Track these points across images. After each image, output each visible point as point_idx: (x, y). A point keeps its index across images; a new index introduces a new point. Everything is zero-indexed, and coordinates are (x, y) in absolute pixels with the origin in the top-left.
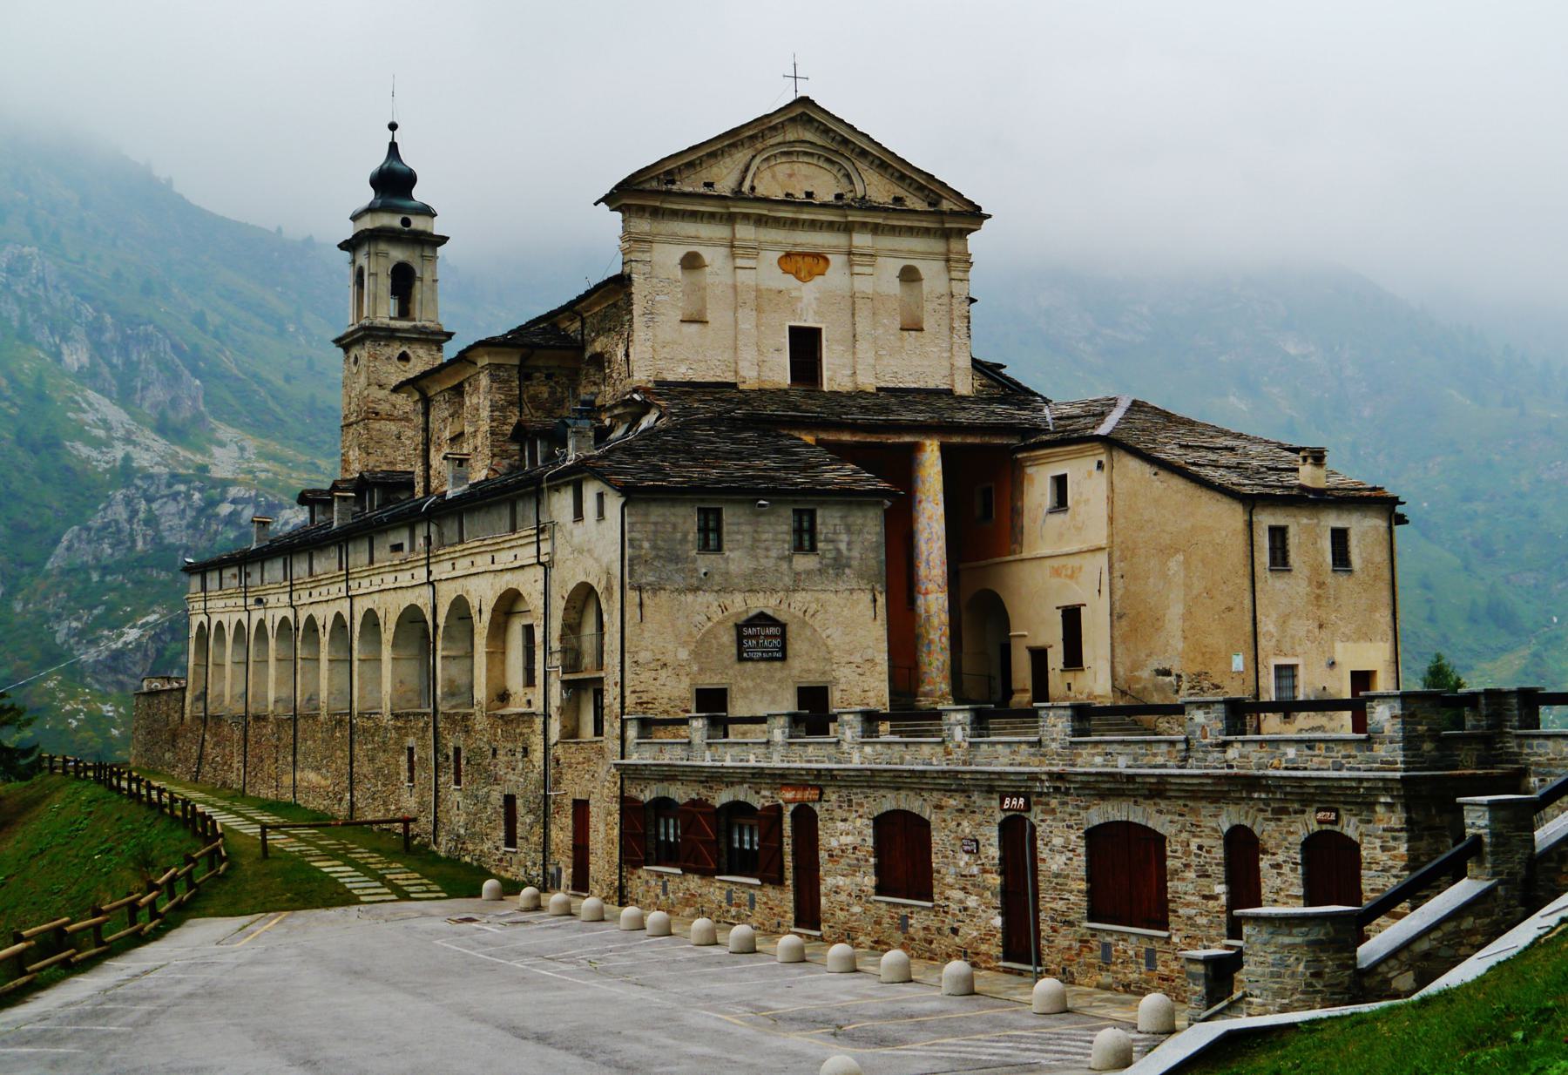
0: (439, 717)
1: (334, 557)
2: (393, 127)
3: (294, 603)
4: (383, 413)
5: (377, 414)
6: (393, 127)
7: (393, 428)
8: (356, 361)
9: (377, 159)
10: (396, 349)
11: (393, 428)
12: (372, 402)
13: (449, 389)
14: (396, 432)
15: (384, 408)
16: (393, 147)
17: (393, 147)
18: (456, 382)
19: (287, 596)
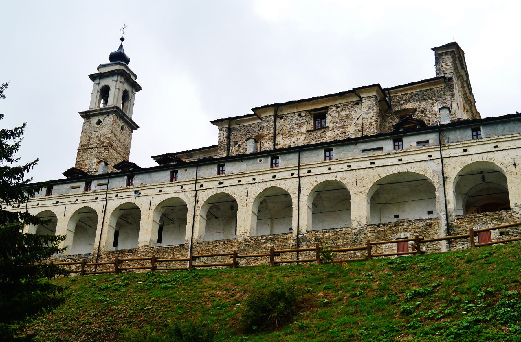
0: (451, 219)
1: (267, 162)
2: (122, 39)
3: (197, 189)
4: (114, 146)
5: (112, 146)
6: (122, 39)
7: (116, 155)
8: (99, 122)
9: (115, 49)
10: (121, 123)
11: (116, 155)
12: (112, 140)
13: (308, 111)
14: (116, 157)
15: (114, 145)
16: (121, 47)
17: (121, 47)
18: (322, 106)
19: (195, 184)
